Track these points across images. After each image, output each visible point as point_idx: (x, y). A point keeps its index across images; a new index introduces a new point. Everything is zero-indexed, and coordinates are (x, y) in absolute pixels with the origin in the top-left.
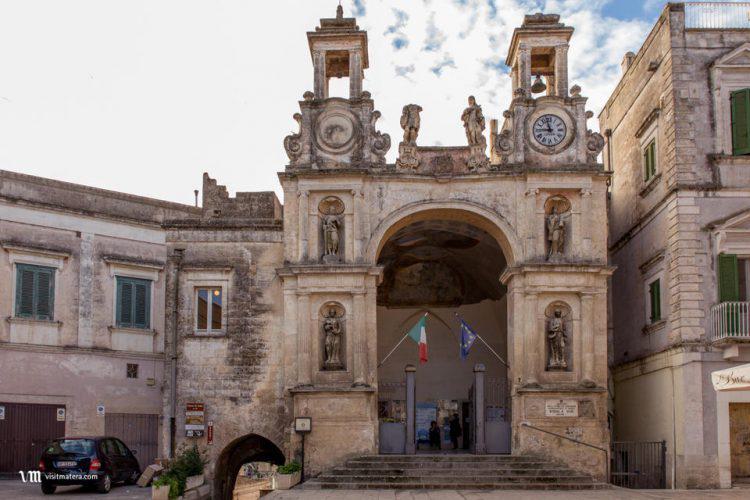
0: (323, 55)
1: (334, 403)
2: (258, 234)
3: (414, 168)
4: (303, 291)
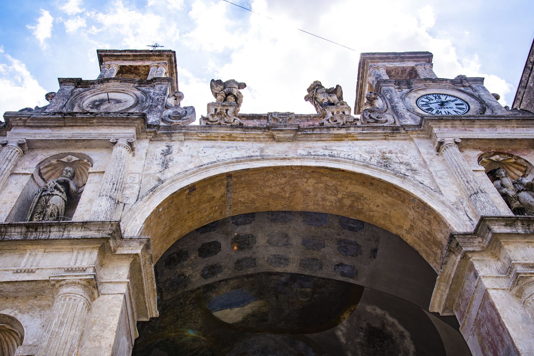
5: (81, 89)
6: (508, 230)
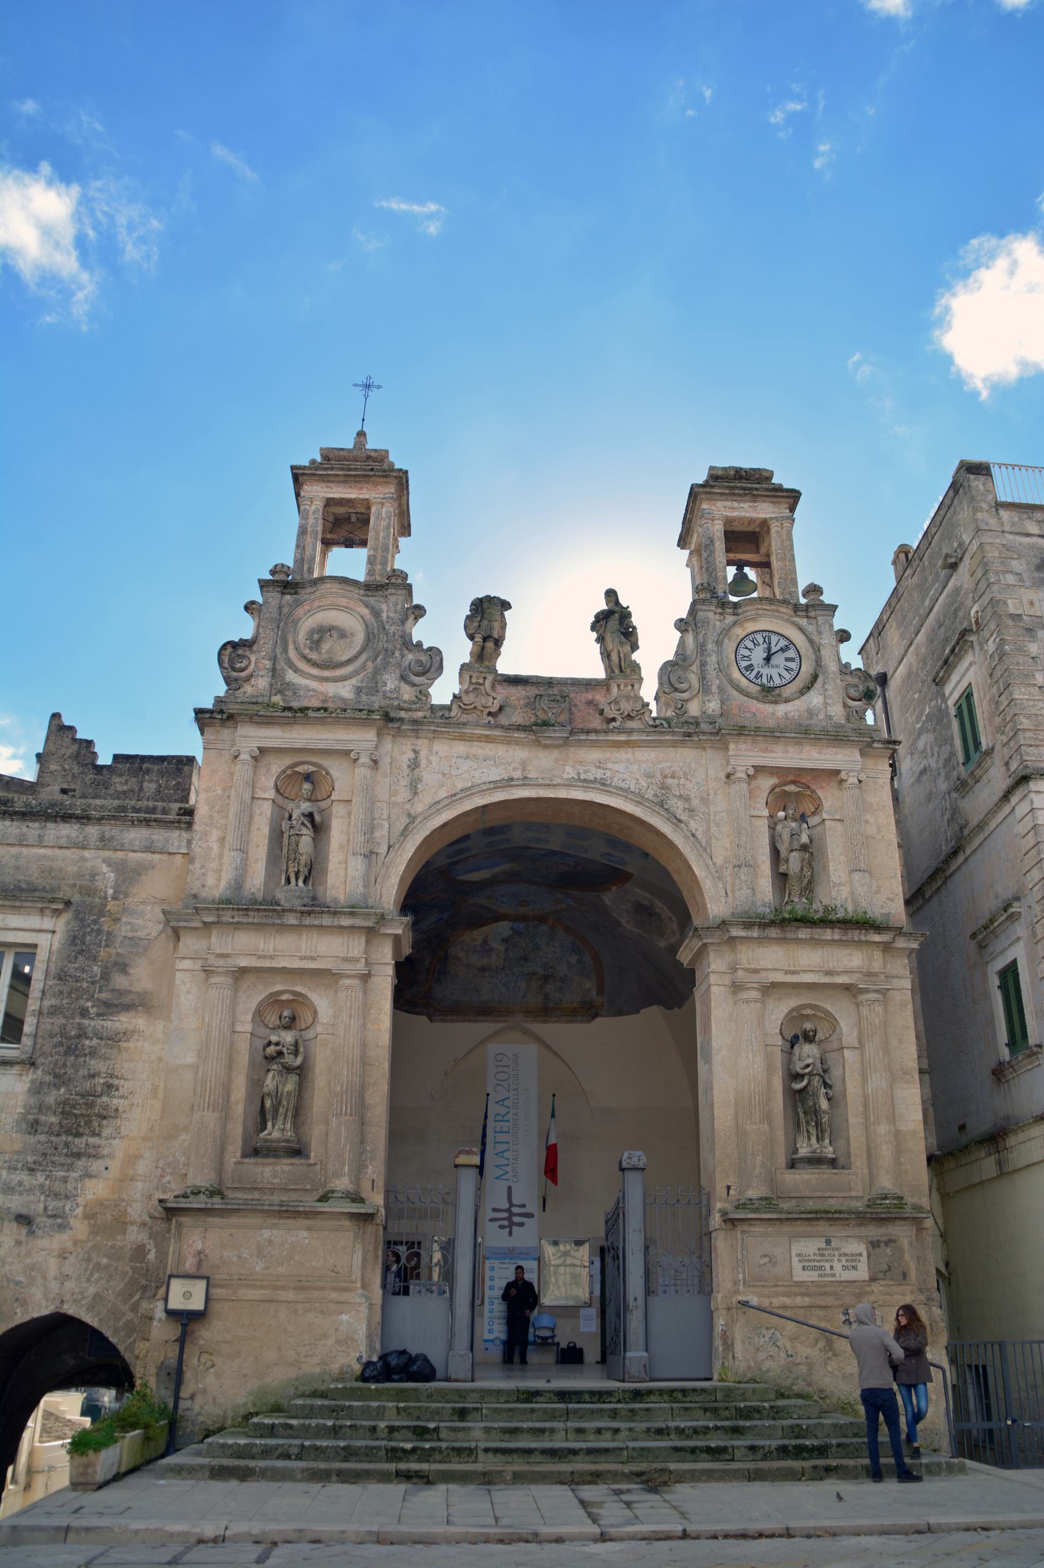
0: (319, 504)
1: (270, 1241)
2: (136, 835)
3: (490, 714)
4: (221, 962)
5: (288, 597)
6: (743, 933)
